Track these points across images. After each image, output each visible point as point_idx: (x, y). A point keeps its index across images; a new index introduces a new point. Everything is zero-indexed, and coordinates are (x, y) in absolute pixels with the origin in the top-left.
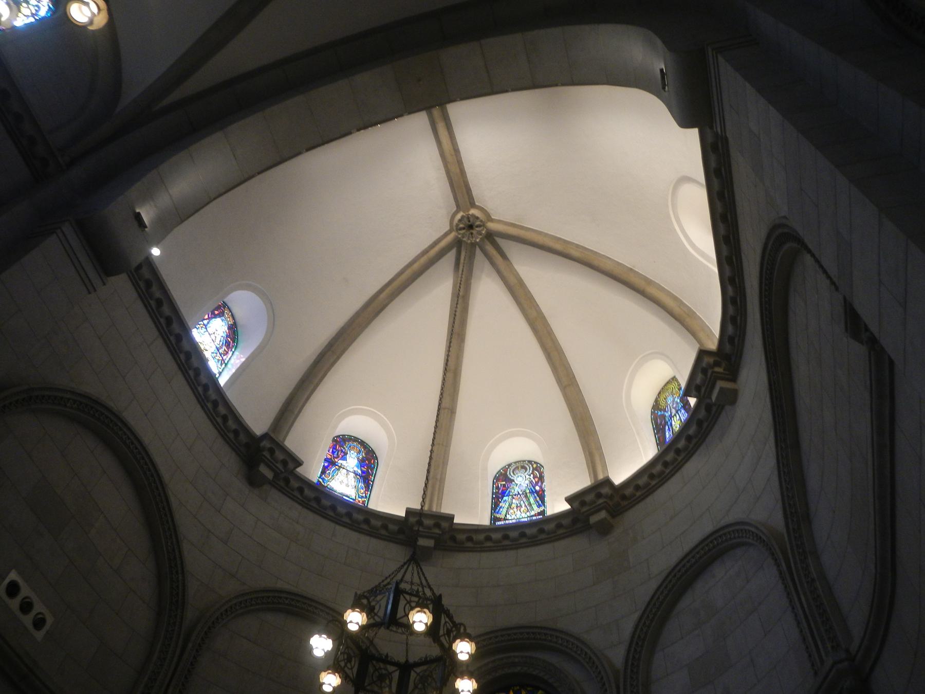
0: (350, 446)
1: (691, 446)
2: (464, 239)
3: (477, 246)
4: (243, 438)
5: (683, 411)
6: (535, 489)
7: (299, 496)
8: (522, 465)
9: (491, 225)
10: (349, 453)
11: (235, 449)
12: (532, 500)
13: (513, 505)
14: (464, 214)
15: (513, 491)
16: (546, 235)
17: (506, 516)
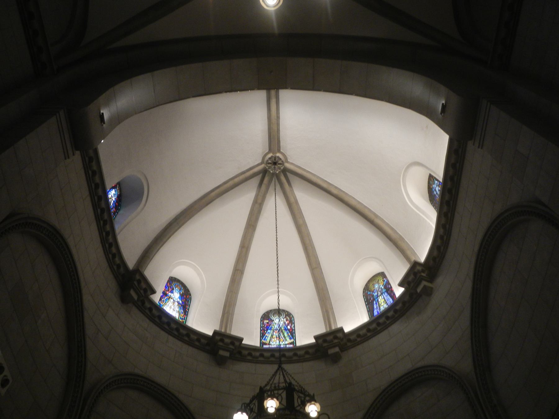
0: (175, 285)
2: (269, 170)
4: (122, 270)
5: (386, 294)
6: (287, 327)
7: (149, 314)
8: (279, 312)
9: (287, 165)
10: (175, 289)
11: (116, 277)
12: (286, 334)
13: (274, 336)
14: (273, 156)
15: (273, 327)
16: (318, 177)
17: (270, 342)
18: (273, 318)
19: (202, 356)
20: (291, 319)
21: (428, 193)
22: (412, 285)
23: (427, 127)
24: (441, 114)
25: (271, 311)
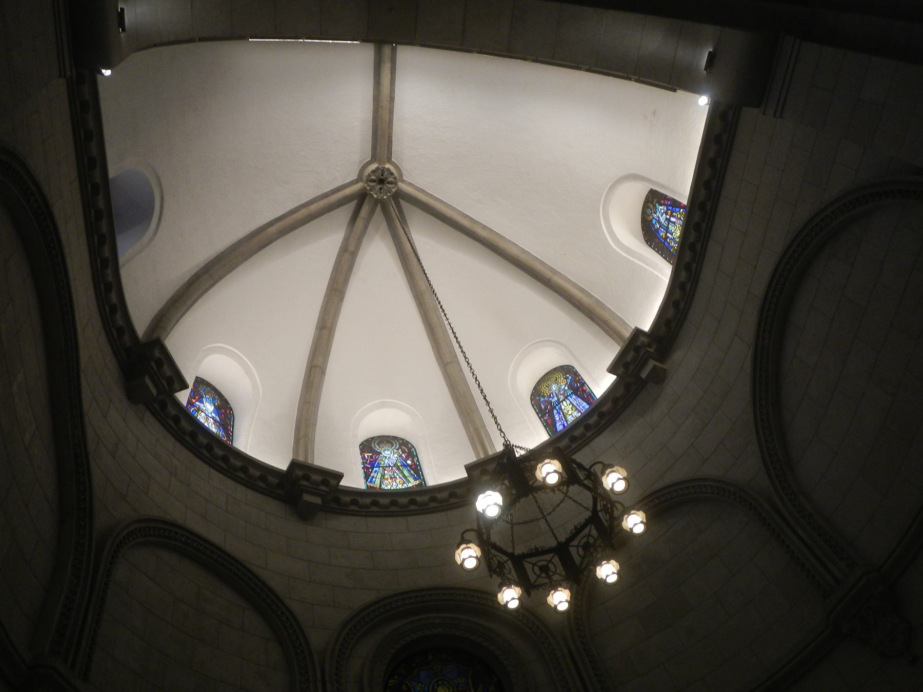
0: (204, 390)
1: (603, 422)
2: (372, 193)
3: (379, 205)
6: (406, 462)
9: (401, 185)
11: (116, 353)
13: (386, 477)
14: (380, 167)
15: (382, 463)
16: (454, 209)
17: (381, 485)
18: (377, 449)
19: (272, 506)
20: (409, 449)
21: (643, 230)
22: (632, 367)
23: (654, 112)
24: (706, 69)
25: (373, 439)
